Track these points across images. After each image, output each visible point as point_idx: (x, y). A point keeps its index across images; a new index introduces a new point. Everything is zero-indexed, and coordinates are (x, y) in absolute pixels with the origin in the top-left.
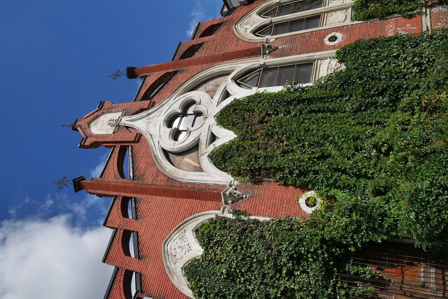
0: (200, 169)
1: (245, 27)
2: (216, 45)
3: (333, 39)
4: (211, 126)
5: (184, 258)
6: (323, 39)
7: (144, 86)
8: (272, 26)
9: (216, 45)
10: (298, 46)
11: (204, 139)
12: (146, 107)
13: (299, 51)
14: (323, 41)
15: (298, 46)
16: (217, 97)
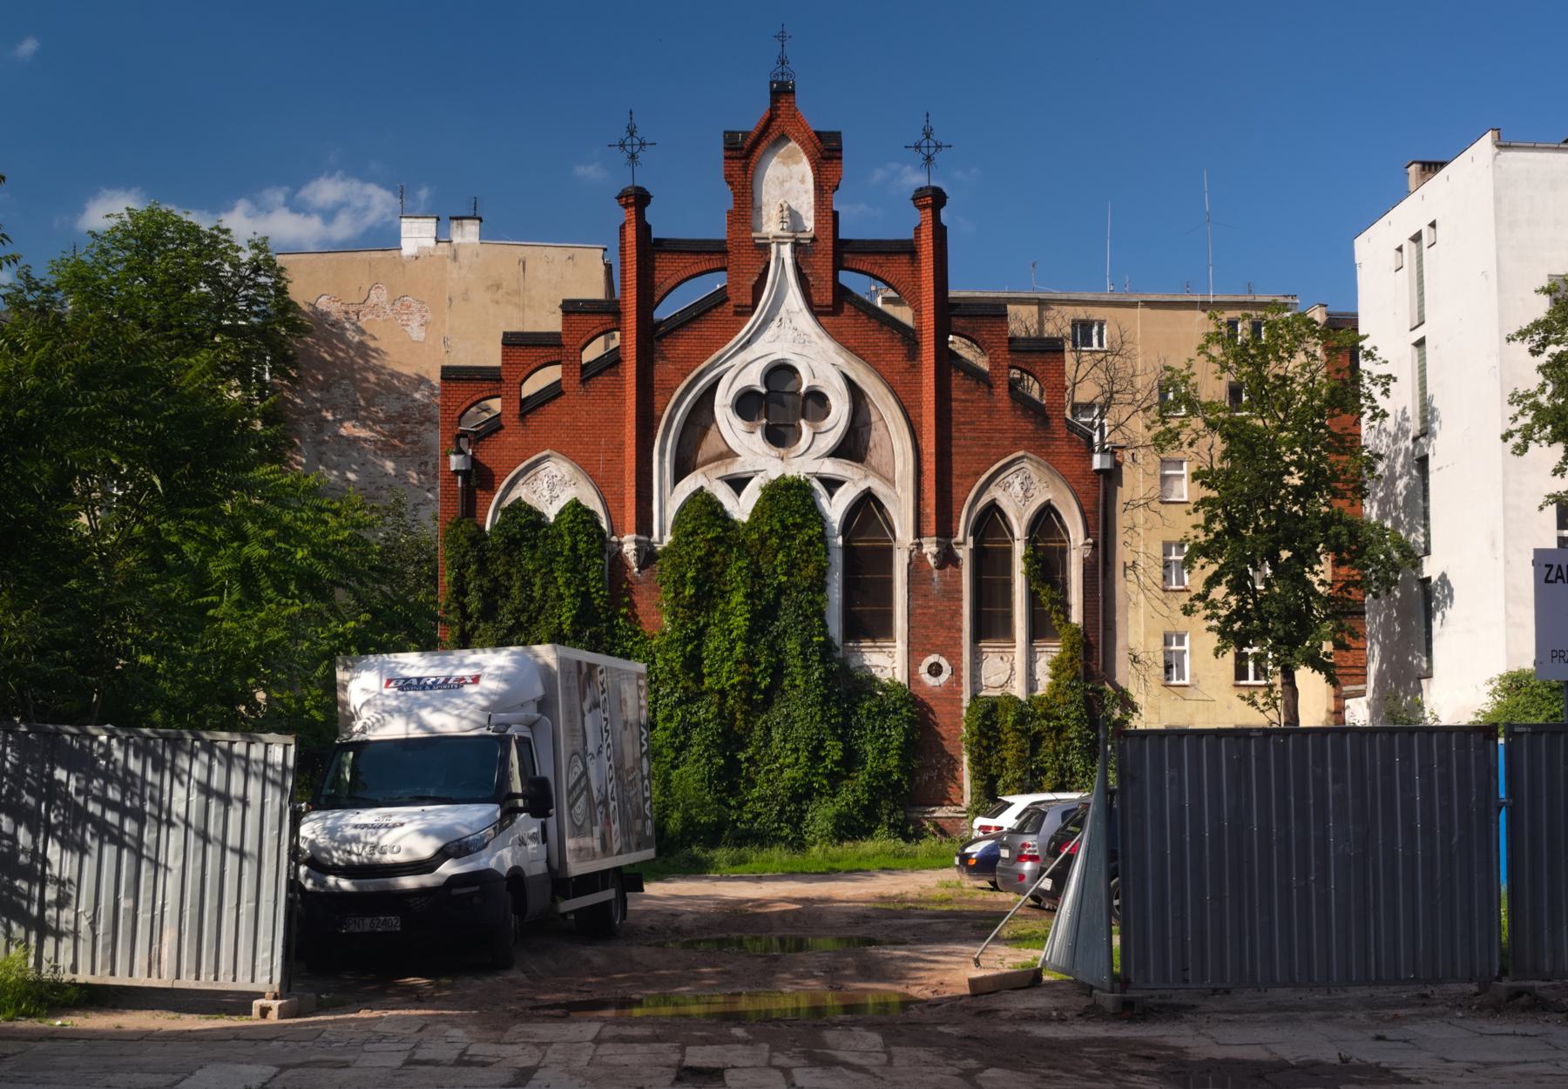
0: (681, 472)
1: (1017, 483)
2: (972, 423)
3: (935, 670)
4: (761, 474)
5: (535, 497)
6: (934, 652)
7: (880, 259)
8: (1009, 542)
9: (972, 423)
10: (931, 607)
11: (736, 468)
12: (816, 300)
13: (918, 611)
14: (931, 652)
15: (931, 607)
16: (830, 468)
